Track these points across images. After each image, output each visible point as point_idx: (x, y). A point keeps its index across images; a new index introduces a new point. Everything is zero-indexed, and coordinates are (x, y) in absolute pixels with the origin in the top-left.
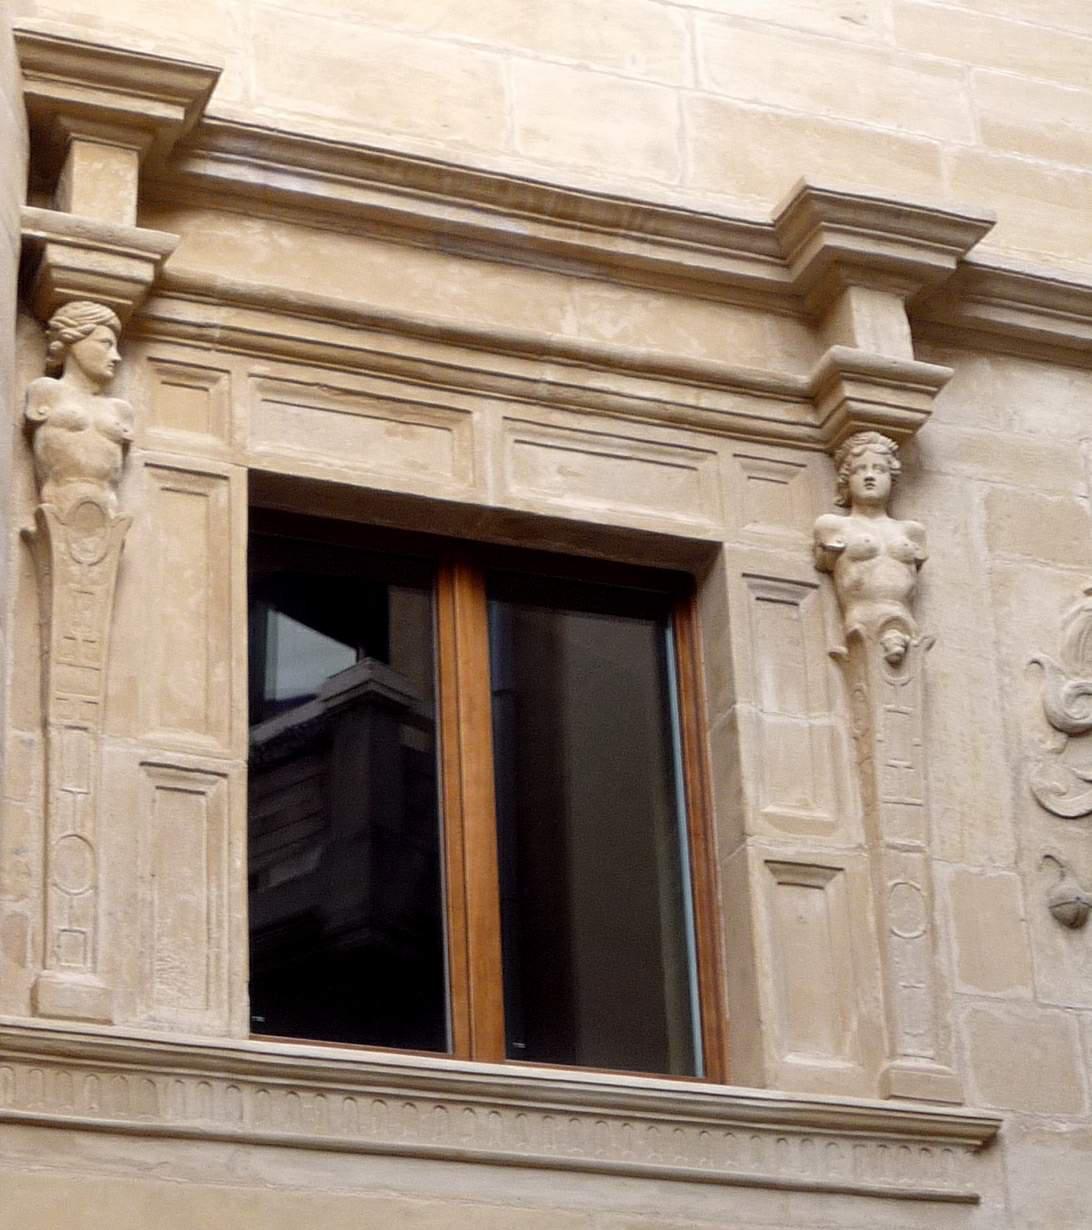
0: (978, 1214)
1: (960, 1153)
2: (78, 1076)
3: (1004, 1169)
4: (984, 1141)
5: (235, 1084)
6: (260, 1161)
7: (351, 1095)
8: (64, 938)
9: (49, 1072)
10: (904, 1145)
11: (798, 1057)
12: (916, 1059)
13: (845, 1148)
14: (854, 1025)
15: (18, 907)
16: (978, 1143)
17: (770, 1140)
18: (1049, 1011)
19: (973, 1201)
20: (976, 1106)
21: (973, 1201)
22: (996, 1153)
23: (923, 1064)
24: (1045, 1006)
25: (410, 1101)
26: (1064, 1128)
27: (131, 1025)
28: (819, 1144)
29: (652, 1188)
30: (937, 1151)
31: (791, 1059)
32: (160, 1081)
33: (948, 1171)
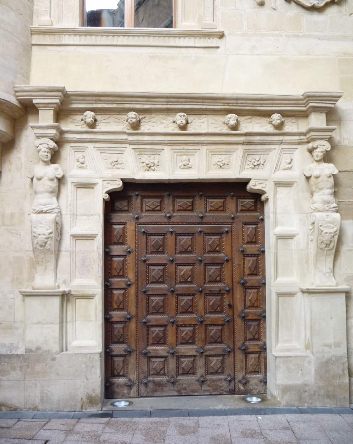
0: (219, 50)
1: (216, 38)
2: (47, 36)
3: (225, 41)
4: (222, 36)
5: (75, 35)
6: (80, 48)
7: (97, 36)
8: (44, 12)
9: (42, 36)
10: (205, 38)
11: (183, 23)
12: (208, 20)
13: (193, 39)
14: (197, 16)
15: (37, 8)
16: (220, 36)
17: (178, 38)
18: (238, 11)
19: (218, 47)
20: (220, 29)
21: (218, 47)
22: (224, 38)
23: (209, 22)
24: (237, 10)
25: (108, 36)
26: (239, 33)
27: (57, 26)
28: (187, 39)
29: (154, 49)
30: (211, 38)
31: (184, 23)
32: (61, 35)
33: (214, 42)
